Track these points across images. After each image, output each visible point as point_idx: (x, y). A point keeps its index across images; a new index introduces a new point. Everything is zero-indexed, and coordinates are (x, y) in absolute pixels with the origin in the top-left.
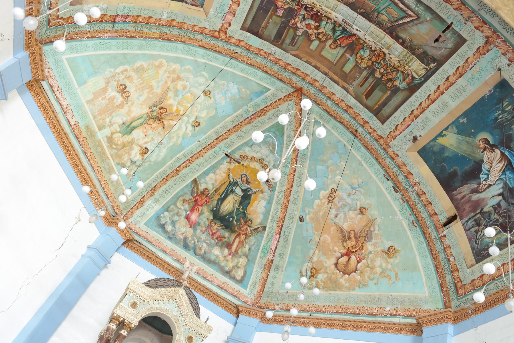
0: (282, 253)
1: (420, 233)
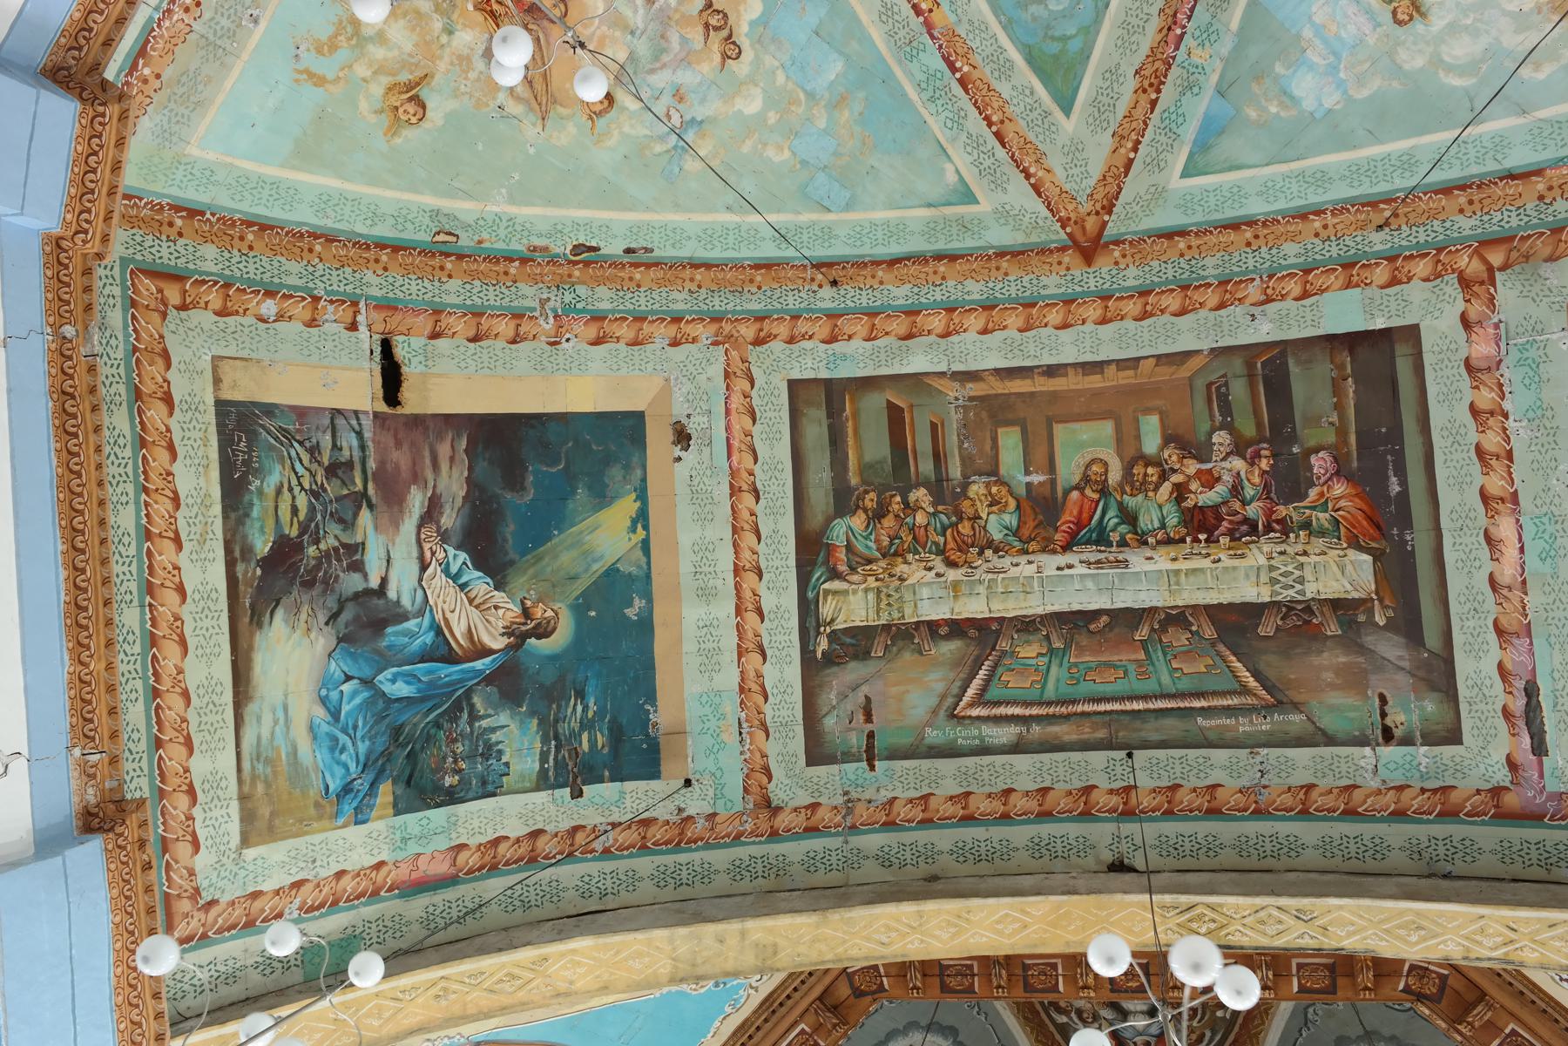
1: (408, 235)
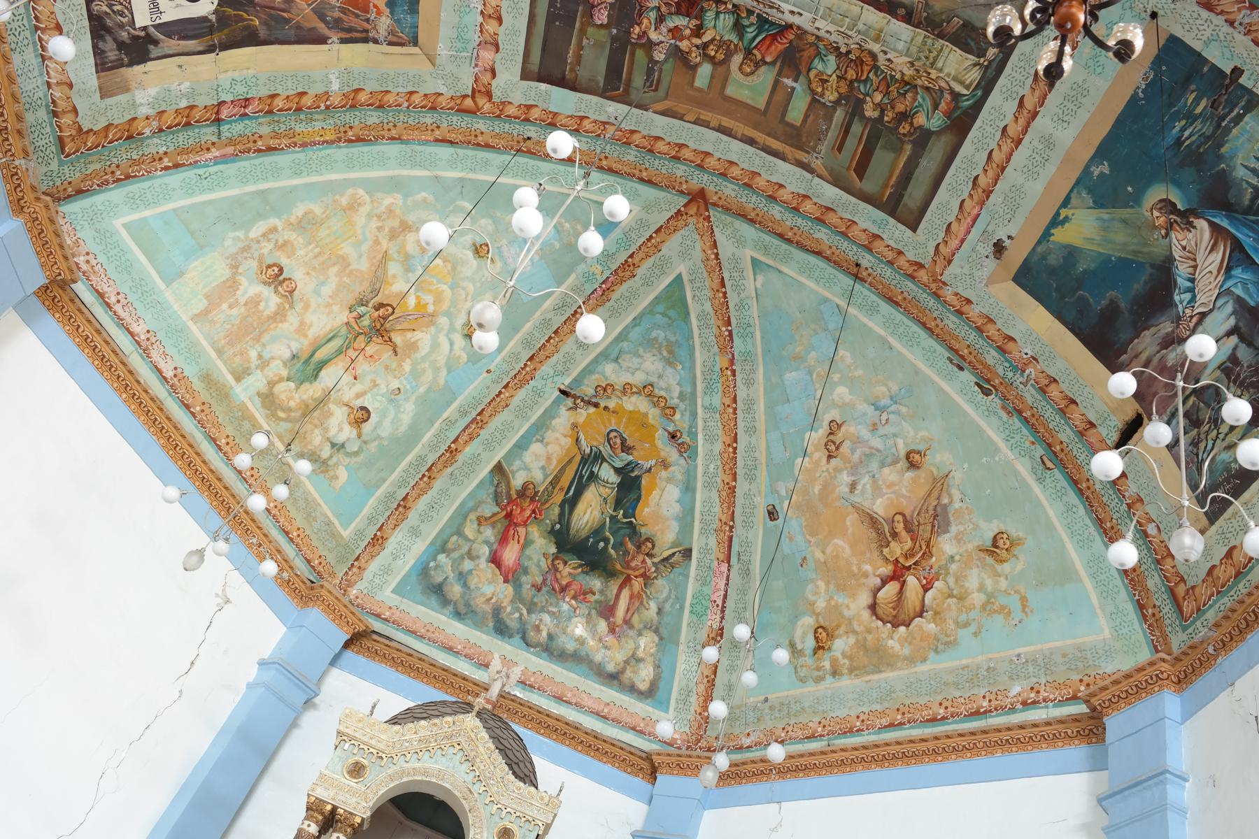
0: (741, 606)
1: (1063, 482)
